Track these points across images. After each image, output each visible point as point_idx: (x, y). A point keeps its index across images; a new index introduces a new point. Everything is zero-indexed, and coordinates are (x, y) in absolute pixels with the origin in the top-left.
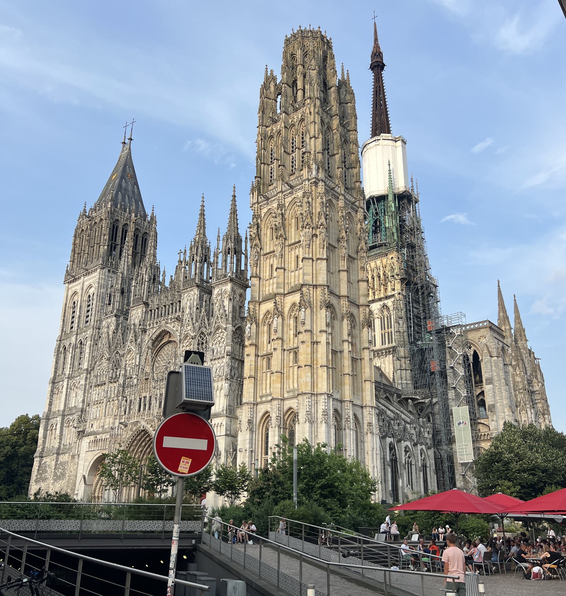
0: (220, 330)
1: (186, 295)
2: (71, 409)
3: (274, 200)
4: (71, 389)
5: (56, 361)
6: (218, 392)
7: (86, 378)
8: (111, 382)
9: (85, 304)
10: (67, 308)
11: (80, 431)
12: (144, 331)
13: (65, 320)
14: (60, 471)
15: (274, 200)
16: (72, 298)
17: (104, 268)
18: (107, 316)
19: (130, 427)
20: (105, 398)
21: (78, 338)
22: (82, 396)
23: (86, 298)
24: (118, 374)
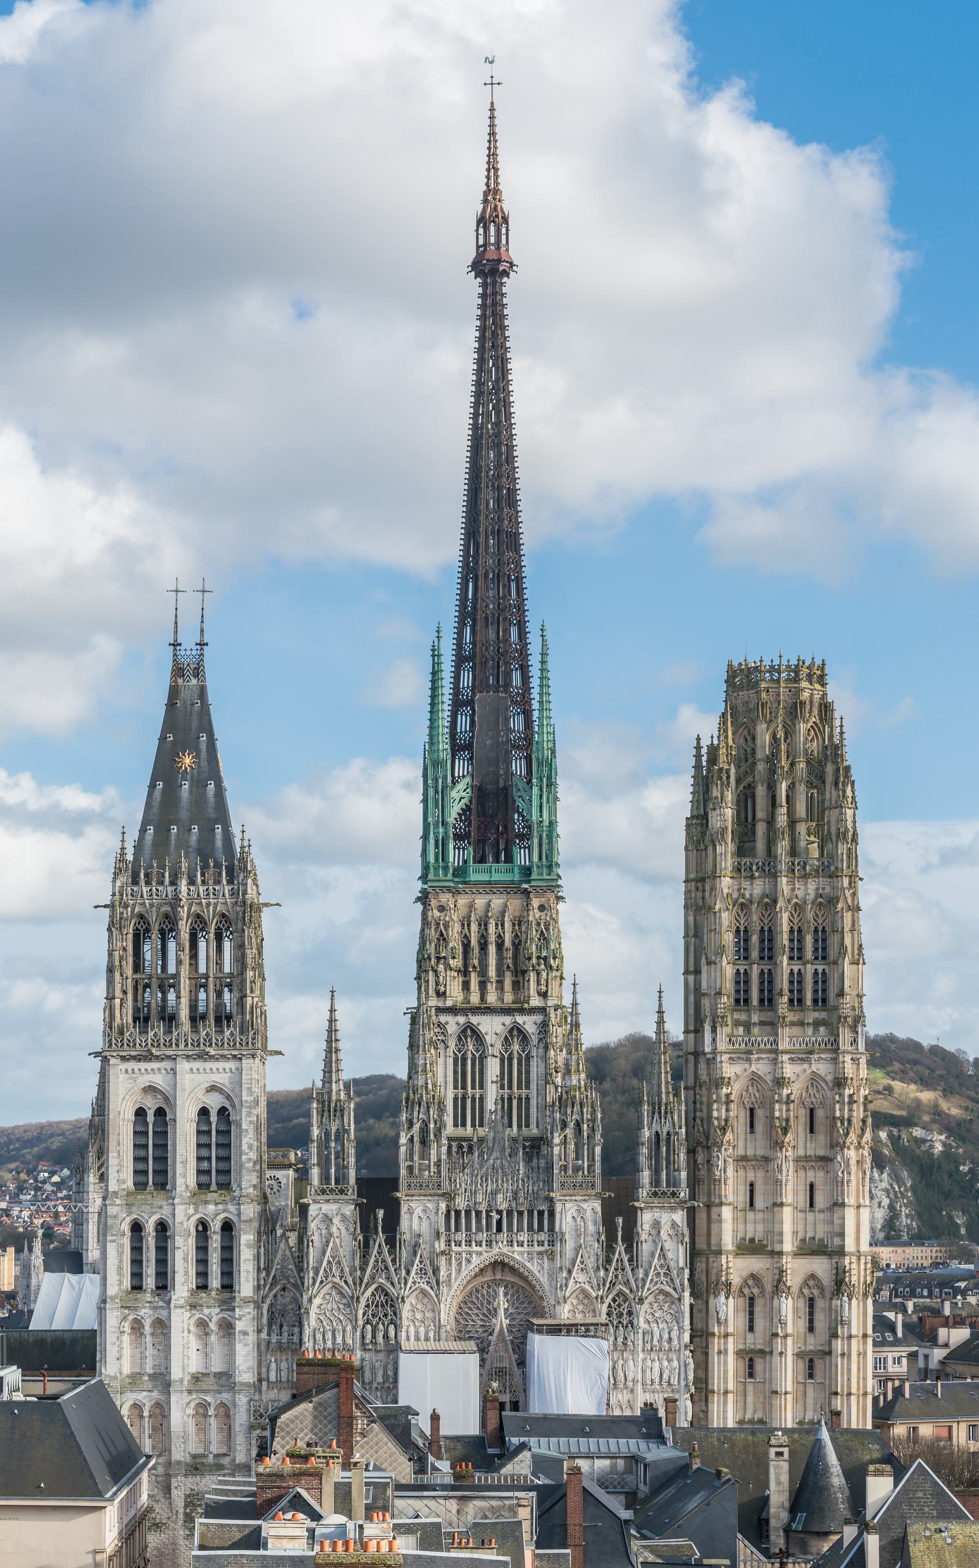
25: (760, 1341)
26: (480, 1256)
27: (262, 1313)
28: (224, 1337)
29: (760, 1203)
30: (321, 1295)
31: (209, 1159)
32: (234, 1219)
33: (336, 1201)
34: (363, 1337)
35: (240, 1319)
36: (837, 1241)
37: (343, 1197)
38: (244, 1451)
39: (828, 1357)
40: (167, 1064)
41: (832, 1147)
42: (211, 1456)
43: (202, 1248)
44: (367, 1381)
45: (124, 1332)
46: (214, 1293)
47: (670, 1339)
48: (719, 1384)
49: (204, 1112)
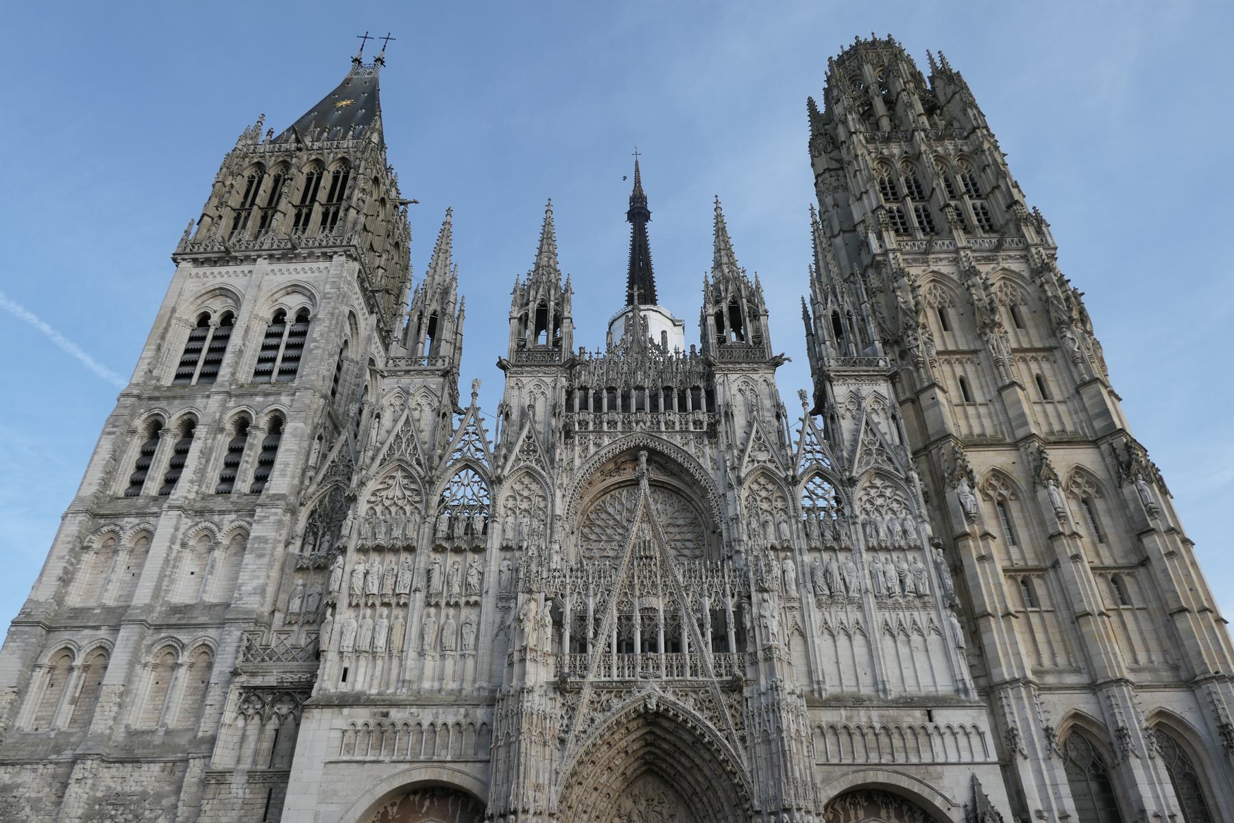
0: (878, 482)
1: (732, 377)
2: (176, 610)
3: (941, 260)
4: (184, 545)
5: (115, 451)
6: (915, 637)
7: (280, 523)
8: (438, 549)
10: (173, 321)
11: (256, 688)
12: (568, 433)
13: (163, 350)
16: (199, 301)
17: (355, 259)
19: (587, 694)
21: (232, 404)
22: (263, 574)
23: (269, 315)
24: (479, 526)
29: (978, 396)
34: (435, 530)
35: (258, 522)
36: (1099, 424)
39: (1142, 570)
40: (246, 267)
42: (161, 732)
43: (236, 450)
44: (432, 591)
47: (905, 532)
48: (993, 602)
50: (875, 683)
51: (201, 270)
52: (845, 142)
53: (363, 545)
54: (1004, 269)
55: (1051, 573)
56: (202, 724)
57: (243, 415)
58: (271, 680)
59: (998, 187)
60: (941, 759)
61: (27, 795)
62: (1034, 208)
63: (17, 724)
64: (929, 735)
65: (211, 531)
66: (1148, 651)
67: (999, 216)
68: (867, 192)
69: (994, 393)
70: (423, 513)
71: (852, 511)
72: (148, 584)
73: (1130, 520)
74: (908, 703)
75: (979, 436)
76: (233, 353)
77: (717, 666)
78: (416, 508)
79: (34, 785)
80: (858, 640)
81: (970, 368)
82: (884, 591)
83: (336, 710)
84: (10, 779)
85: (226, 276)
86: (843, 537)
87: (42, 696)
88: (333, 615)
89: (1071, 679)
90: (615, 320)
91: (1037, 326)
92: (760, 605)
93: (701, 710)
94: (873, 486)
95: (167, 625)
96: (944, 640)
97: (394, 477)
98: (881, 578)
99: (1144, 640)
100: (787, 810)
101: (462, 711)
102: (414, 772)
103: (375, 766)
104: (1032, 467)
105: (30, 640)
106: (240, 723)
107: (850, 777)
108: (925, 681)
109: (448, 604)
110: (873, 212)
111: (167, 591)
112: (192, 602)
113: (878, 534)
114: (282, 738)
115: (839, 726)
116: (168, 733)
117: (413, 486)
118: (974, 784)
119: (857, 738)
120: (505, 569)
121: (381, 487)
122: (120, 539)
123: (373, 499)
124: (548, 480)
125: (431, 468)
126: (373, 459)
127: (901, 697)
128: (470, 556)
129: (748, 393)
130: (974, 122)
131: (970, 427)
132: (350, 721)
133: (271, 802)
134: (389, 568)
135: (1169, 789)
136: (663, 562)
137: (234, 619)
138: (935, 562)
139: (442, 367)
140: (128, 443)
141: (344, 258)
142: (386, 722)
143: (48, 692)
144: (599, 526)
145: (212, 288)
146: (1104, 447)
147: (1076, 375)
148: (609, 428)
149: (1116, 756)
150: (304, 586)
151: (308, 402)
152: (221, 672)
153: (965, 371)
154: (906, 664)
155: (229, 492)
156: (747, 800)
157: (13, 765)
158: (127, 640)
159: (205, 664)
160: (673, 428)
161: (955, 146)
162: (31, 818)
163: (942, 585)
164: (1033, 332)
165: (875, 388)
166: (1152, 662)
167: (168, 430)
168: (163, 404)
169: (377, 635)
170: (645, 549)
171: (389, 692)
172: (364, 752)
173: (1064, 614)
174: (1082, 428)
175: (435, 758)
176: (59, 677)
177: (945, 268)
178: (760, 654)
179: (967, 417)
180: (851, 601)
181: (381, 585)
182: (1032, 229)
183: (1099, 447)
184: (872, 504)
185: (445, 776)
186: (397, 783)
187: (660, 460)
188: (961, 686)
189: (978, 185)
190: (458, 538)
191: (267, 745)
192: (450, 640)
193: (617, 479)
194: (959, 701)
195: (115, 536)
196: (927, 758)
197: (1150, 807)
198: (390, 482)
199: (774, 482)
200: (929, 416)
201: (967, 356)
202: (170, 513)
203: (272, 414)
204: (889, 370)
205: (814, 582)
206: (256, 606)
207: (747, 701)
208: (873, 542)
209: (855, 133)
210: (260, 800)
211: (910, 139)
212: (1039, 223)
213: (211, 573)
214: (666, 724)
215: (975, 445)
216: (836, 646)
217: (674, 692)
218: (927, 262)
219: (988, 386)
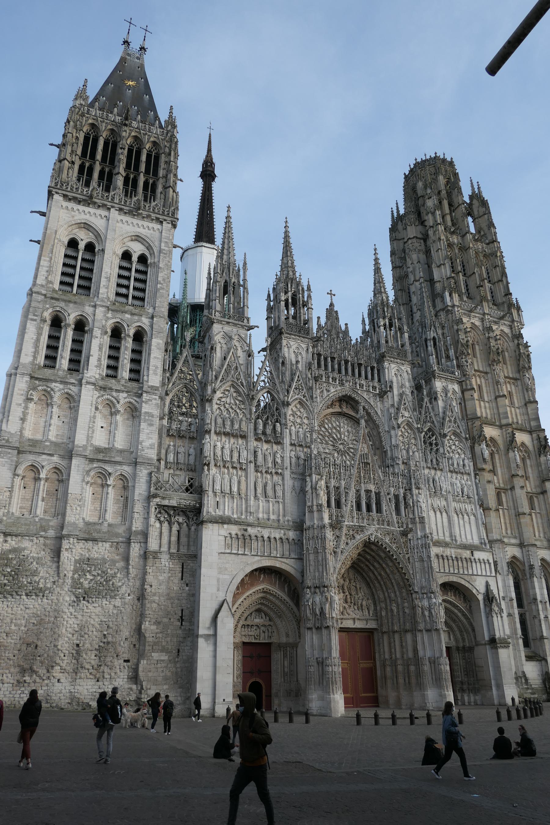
0: (453, 437)
1: (393, 366)
2: (99, 450)
3: (476, 317)
4: (97, 409)
6: (466, 516)
8: (258, 439)
9: (117, 261)
10: (56, 241)
14: (89, 576)
15: (476, 317)
16: (70, 229)
18: (228, 320)
19: (344, 530)
20: (251, 462)
23: (120, 252)
25: (501, 482)
26: (335, 391)
27: (164, 404)
28: (128, 419)
30: (222, 389)
31: (127, 287)
32: (147, 328)
33: (235, 325)
34: (255, 429)
35: (146, 403)
36: (533, 424)
37: (242, 323)
38: (141, 520)
39: (541, 496)
40: (104, 213)
41: (519, 371)
43: (115, 348)
44: (258, 464)
45: (32, 399)
46: (123, 382)
47: (464, 465)
49: (126, 256)
50: (451, 536)
51: (71, 205)
52: (433, 227)
53: (220, 431)
54: (501, 330)
55: (509, 492)
56: (134, 523)
57: (117, 324)
58: (174, 503)
59: (501, 281)
60: (475, 573)
61: (31, 555)
62: (516, 299)
63: (11, 510)
64: (471, 562)
65: (112, 402)
66: (539, 532)
67: (500, 299)
68: (444, 264)
69: (493, 397)
70: (249, 416)
71: (444, 451)
72: (82, 432)
73: (540, 472)
74: (465, 547)
75: (485, 418)
76: (107, 278)
77: (398, 523)
78: (243, 412)
79: (34, 550)
80: (444, 514)
81: (483, 380)
82: (456, 493)
83: (220, 525)
84: (16, 544)
85: (88, 214)
86: (440, 464)
87: (21, 494)
88: (208, 470)
89: (513, 541)
90: (190, 249)
91: (511, 365)
92: (417, 496)
93: (391, 543)
94: (451, 439)
95: (97, 459)
96: (476, 519)
97: (227, 390)
98: (455, 487)
99: (538, 527)
100: (432, 593)
101: (282, 531)
102: (263, 561)
103: (244, 557)
104: (508, 439)
105: (12, 459)
106: (158, 525)
107: (444, 578)
108: (469, 537)
109: (266, 472)
110: (447, 279)
111: (92, 437)
112: (107, 446)
113: (453, 465)
114: (182, 535)
115: (440, 555)
116: (110, 525)
117: (239, 398)
118: (487, 585)
119: (446, 561)
120: (293, 456)
121: (222, 395)
122: (52, 397)
123: (218, 402)
124: (312, 410)
125: (250, 390)
126: (216, 378)
127: (461, 544)
128: (275, 447)
129: (399, 376)
130: (494, 237)
131: (482, 413)
132: (228, 532)
133: (184, 570)
134: (234, 446)
135: (545, 591)
136: (373, 466)
137: (142, 463)
138: (476, 482)
139: (248, 325)
140: (42, 328)
141: (170, 225)
142: (246, 534)
143: (24, 492)
144: (321, 434)
145: (79, 222)
146: (534, 435)
147: (526, 396)
148: (332, 381)
149: (526, 575)
150: (174, 446)
151: (162, 326)
152: (140, 494)
153: (481, 382)
154: (462, 528)
155: (115, 377)
156: (410, 586)
157: (16, 536)
158: (78, 466)
159: (121, 486)
160: (362, 388)
161: (483, 248)
162: (39, 569)
163: (477, 494)
164: (509, 367)
165: (453, 387)
166: (540, 537)
167: (69, 325)
168: (62, 304)
169: (233, 485)
170: (367, 459)
171: (243, 517)
172: (237, 549)
173: (513, 511)
174: (525, 423)
175: (272, 555)
176: (28, 483)
177: (478, 323)
178: (417, 519)
179: (480, 407)
180: (443, 496)
181: (231, 457)
182: (516, 311)
183: (531, 435)
184: (451, 448)
185: (278, 564)
186: (255, 567)
187: (353, 404)
188: (483, 541)
189: (490, 275)
190: (270, 435)
191: (174, 539)
192: (270, 492)
193: (331, 410)
194: (483, 548)
195: (48, 394)
196: (470, 572)
197: (539, 598)
198: (227, 393)
199: (411, 429)
200: (469, 404)
201: (483, 374)
202: (87, 386)
203: (137, 328)
204: (460, 378)
205: (429, 485)
206: (153, 456)
207: (410, 540)
208: (452, 469)
209: (440, 224)
210: (178, 569)
211: (463, 236)
212: (519, 309)
213: (116, 429)
214: (373, 547)
215: (485, 424)
216: (436, 517)
217: (381, 534)
218: (470, 316)
219: (490, 393)
